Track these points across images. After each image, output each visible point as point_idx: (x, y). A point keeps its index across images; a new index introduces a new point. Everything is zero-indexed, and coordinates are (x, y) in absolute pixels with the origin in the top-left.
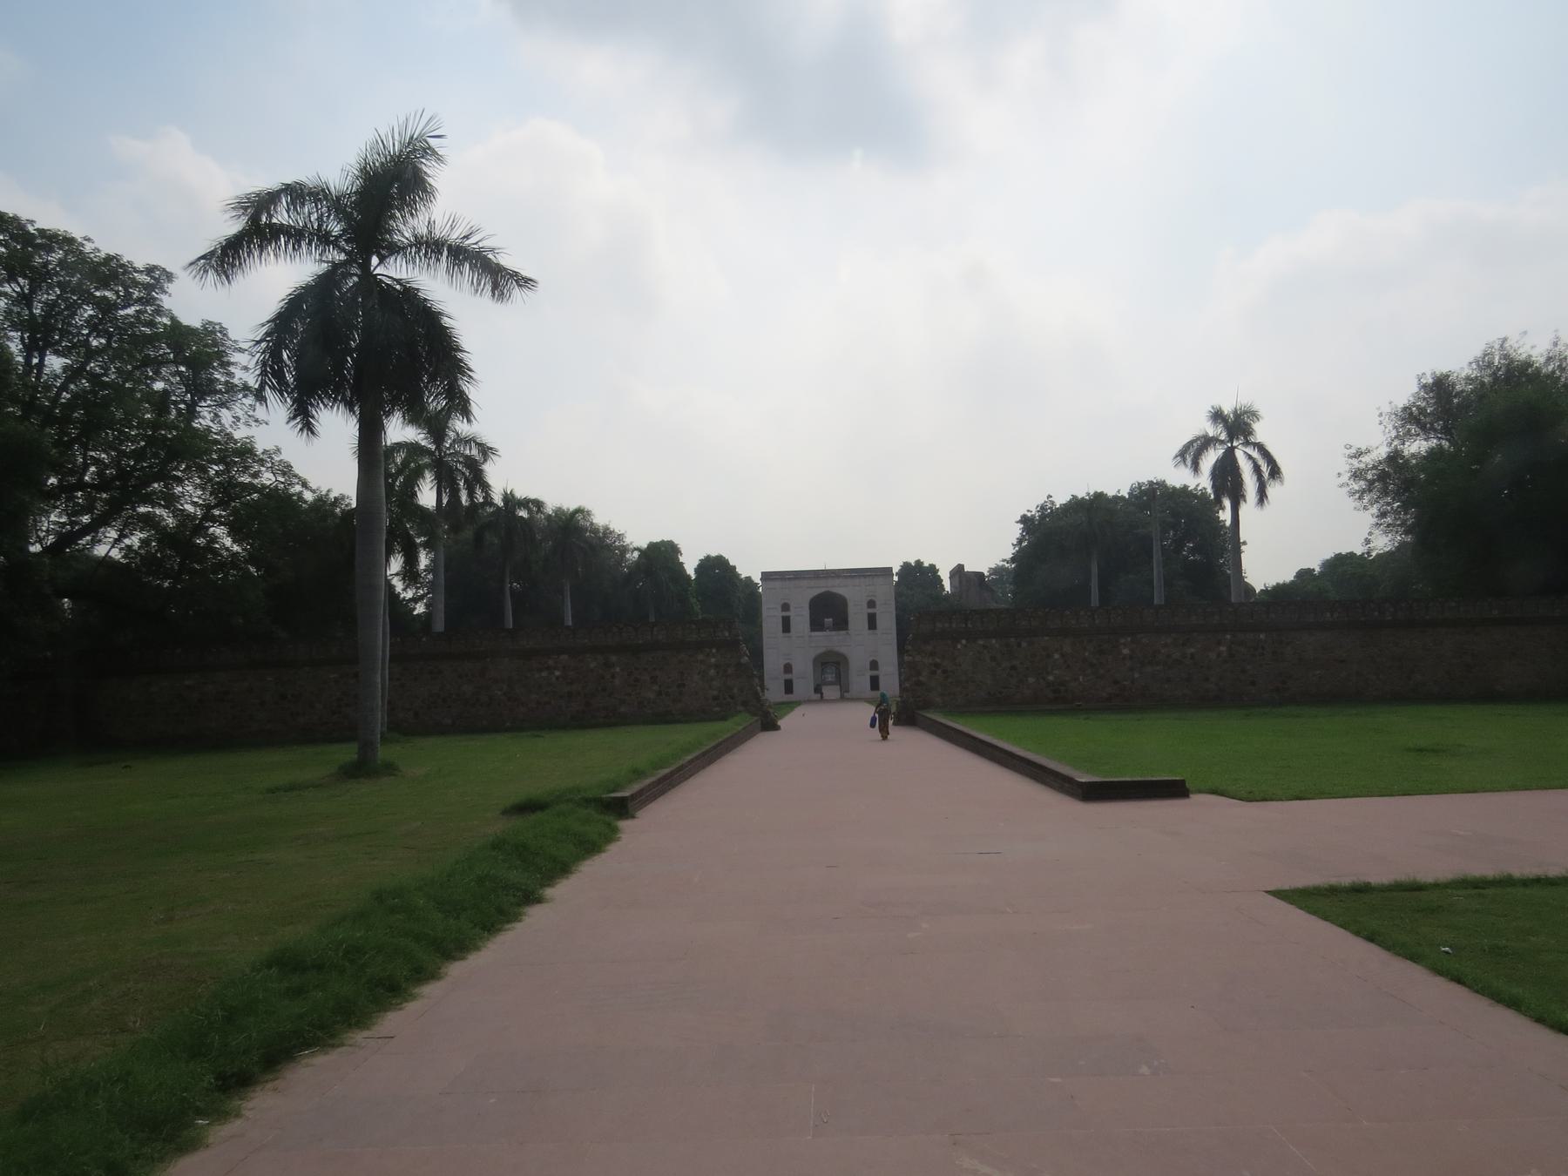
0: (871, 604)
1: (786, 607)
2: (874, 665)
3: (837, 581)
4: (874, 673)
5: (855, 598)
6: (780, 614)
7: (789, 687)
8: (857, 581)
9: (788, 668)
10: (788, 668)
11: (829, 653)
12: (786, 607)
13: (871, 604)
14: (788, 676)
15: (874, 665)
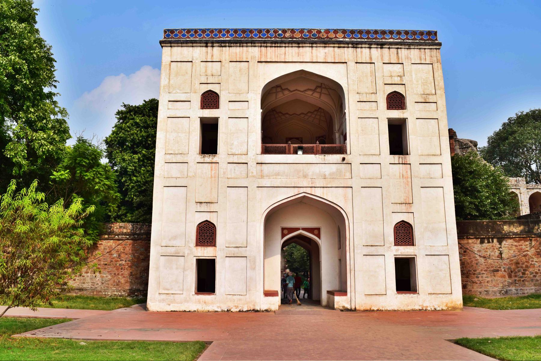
0: (396, 100)
1: (210, 99)
2: (404, 233)
3: (321, 52)
4: (405, 251)
5: (360, 79)
6: (198, 113)
7: (206, 278)
8: (364, 53)
9: (206, 233)
10: (206, 233)
11: (303, 203)
12: (210, 99)
13: (396, 100)
14: (206, 253)
15: (404, 233)
